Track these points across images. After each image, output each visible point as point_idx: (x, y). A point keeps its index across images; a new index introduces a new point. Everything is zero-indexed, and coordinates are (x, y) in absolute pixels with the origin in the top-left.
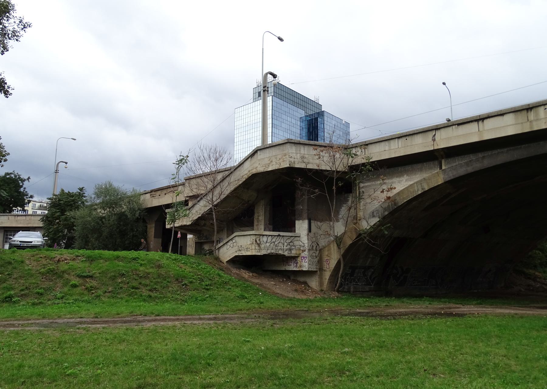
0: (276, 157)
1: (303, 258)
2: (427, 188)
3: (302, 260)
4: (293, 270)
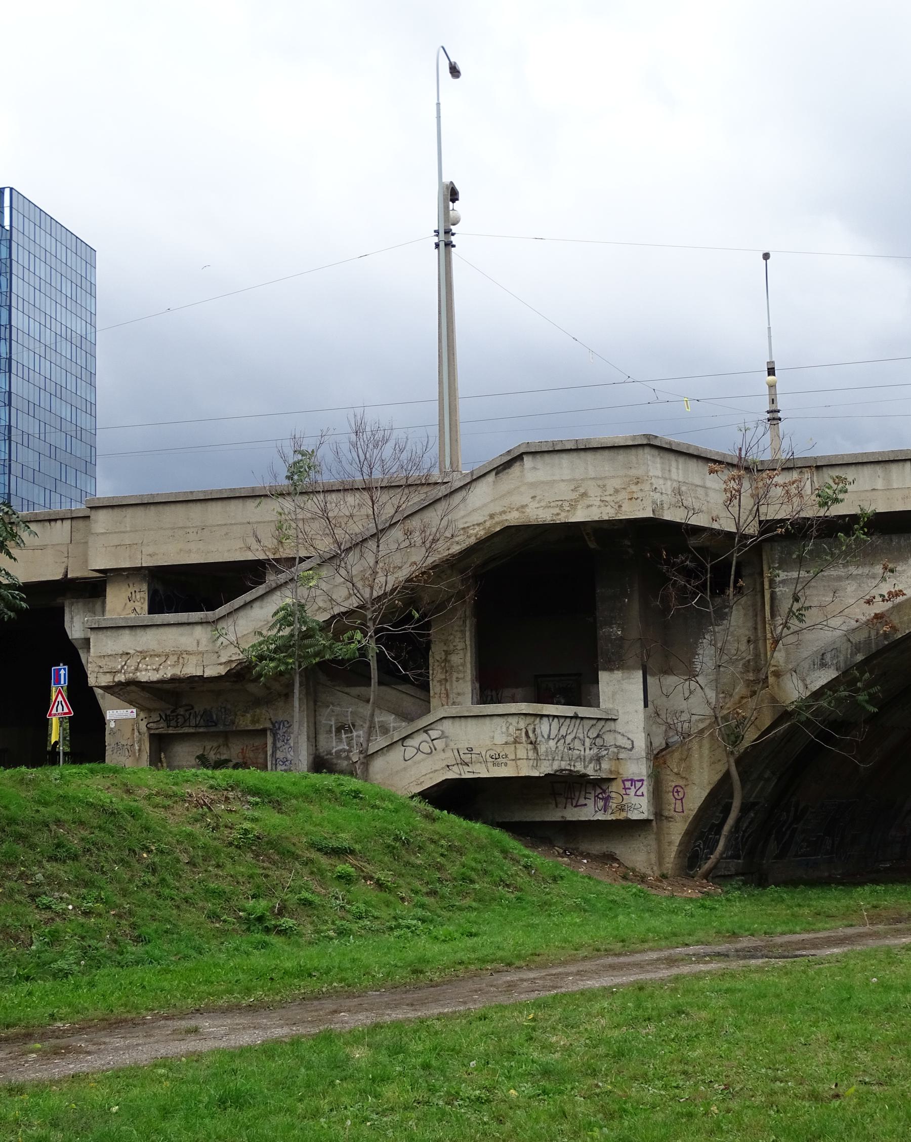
0: (600, 483)
1: (628, 784)
3: (625, 789)
4: (595, 818)
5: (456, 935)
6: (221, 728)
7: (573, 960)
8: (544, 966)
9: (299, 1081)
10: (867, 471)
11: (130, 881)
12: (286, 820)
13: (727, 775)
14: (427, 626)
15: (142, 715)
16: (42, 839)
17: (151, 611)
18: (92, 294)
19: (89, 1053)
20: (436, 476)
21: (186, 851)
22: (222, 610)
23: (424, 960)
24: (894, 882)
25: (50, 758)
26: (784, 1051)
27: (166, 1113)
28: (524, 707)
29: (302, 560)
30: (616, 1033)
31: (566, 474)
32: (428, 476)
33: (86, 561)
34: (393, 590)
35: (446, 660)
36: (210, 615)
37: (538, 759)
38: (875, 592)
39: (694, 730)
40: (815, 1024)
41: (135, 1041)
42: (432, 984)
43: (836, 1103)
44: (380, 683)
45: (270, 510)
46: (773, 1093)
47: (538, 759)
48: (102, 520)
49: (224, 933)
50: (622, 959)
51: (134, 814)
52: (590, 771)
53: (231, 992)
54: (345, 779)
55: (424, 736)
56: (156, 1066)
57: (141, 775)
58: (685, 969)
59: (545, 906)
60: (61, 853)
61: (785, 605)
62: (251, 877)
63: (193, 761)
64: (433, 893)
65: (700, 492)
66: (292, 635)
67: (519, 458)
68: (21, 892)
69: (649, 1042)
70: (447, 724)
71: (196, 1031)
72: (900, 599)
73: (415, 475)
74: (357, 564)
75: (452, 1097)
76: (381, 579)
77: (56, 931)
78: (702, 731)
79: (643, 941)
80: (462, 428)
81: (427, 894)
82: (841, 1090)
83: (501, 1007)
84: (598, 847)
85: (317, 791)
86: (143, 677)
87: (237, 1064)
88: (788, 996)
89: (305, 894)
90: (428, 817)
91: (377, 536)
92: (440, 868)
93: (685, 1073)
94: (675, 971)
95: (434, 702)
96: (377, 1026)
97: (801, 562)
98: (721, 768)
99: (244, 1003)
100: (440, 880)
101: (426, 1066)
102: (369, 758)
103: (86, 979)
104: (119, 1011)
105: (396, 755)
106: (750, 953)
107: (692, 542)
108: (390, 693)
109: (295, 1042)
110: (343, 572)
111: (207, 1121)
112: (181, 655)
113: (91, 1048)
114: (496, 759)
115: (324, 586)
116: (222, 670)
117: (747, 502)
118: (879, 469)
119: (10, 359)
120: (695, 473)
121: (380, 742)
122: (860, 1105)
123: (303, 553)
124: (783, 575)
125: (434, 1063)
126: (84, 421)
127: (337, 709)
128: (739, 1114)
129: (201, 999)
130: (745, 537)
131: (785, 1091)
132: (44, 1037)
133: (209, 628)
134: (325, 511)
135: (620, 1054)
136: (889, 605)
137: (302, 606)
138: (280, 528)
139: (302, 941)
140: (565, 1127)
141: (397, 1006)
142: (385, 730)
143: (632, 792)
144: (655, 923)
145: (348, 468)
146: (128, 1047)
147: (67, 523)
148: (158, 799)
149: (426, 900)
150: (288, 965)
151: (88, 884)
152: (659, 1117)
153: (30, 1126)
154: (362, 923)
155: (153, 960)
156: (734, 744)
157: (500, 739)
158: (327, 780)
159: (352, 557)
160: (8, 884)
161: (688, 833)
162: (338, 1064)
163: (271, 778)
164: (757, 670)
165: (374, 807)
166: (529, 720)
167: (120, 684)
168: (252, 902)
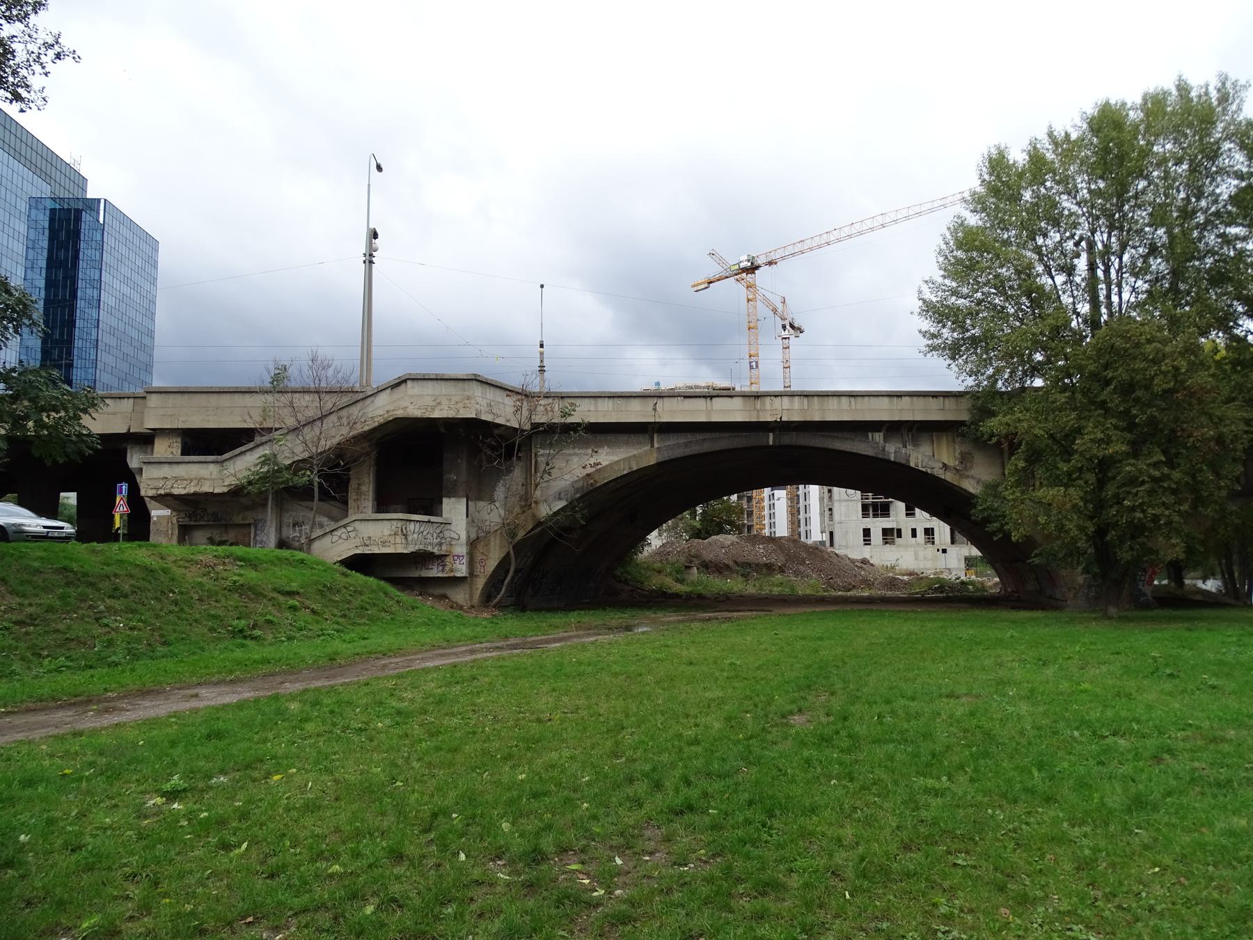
2: (635, 468)
5: (356, 639)
6: (223, 522)
7: (420, 652)
8: (404, 655)
9: (256, 723)
10: (586, 401)
11: (161, 610)
12: (260, 576)
13: (508, 554)
14: (349, 469)
15: (174, 514)
16: (105, 585)
17: (183, 454)
18: (155, 267)
19: (128, 710)
20: (357, 387)
21: (197, 592)
22: (226, 456)
23: (336, 653)
24: (589, 609)
25: (115, 537)
26: (525, 697)
27: (173, 744)
28: (400, 516)
29: (276, 429)
30: (439, 691)
31: (430, 391)
32: (353, 387)
33: (142, 423)
34: (329, 449)
35: (358, 489)
36: (219, 458)
37: (407, 544)
38: (587, 463)
39: (492, 530)
40: (543, 683)
41: (158, 703)
42: (340, 666)
43: (549, 723)
44: (320, 500)
45: (259, 400)
46: (518, 720)
47: (407, 544)
48: (154, 400)
49: (219, 639)
50: (446, 651)
51: (165, 571)
52: (436, 551)
53: (220, 673)
54: (296, 553)
55: (344, 530)
56: (170, 717)
57: (171, 548)
58: (479, 656)
59: (407, 623)
60: (117, 594)
61: (542, 467)
62: (237, 607)
63: (205, 541)
64: (344, 616)
65: (502, 406)
66: (268, 471)
67: (405, 381)
68: (89, 616)
69: (456, 695)
70: (357, 523)
71: (197, 695)
72: (599, 467)
73: (345, 386)
74: (309, 434)
75: (347, 728)
76: (323, 442)
77: (112, 639)
78: (496, 531)
79: (459, 641)
80: (374, 362)
81: (341, 617)
82: (552, 717)
83: (378, 678)
84: (438, 591)
85: (279, 559)
86: (176, 492)
87: (221, 714)
88: (531, 669)
89: (269, 617)
90: (343, 574)
91: (321, 418)
92: (349, 602)
93: (474, 711)
94: (474, 657)
95: (350, 511)
96: (306, 690)
97: (551, 446)
98: (505, 551)
99: (228, 679)
100: (348, 609)
101: (332, 712)
102: (311, 541)
103: (129, 667)
104: (150, 685)
105: (327, 540)
106: (515, 647)
107: (496, 432)
108: (325, 505)
109: (257, 700)
110: (300, 437)
111: (199, 747)
112: (200, 480)
113: (129, 707)
114: (384, 543)
115: (289, 445)
116: (226, 490)
117: (525, 413)
118: (592, 401)
119: (99, 300)
120: (499, 396)
121: (318, 532)
122: (561, 724)
123: (277, 426)
124: (542, 452)
125: (336, 710)
126: (146, 340)
127: (294, 513)
128: (500, 731)
129: (201, 677)
130: (523, 431)
131: (524, 718)
132: (99, 702)
133: (218, 466)
134: (291, 403)
135: (440, 702)
136: (593, 469)
137: (275, 456)
138: (264, 411)
139: (266, 643)
140: (407, 742)
141: (319, 679)
142: (321, 526)
143: (458, 562)
144: (466, 631)
145: (307, 380)
146: (153, 706)
147: (131, 401)
148: (181, 563)
149: (341, 620)
150: (256, 657)
151: (133, 611)
152: (458, 734)
153: (85, 755)
154: (301, 633)
155: (173, 655)
156: (513, 538)
157: (387, 532)
158: (285, 553)
159: (306, 430)
160: (80, 612)
161: (486, 584)
162: (280, 712)
163: (253, 551)
164: (526, 500)
165: (312, 568)
166: (404, 522)
167: (161, 495)
168: (236, 622)
